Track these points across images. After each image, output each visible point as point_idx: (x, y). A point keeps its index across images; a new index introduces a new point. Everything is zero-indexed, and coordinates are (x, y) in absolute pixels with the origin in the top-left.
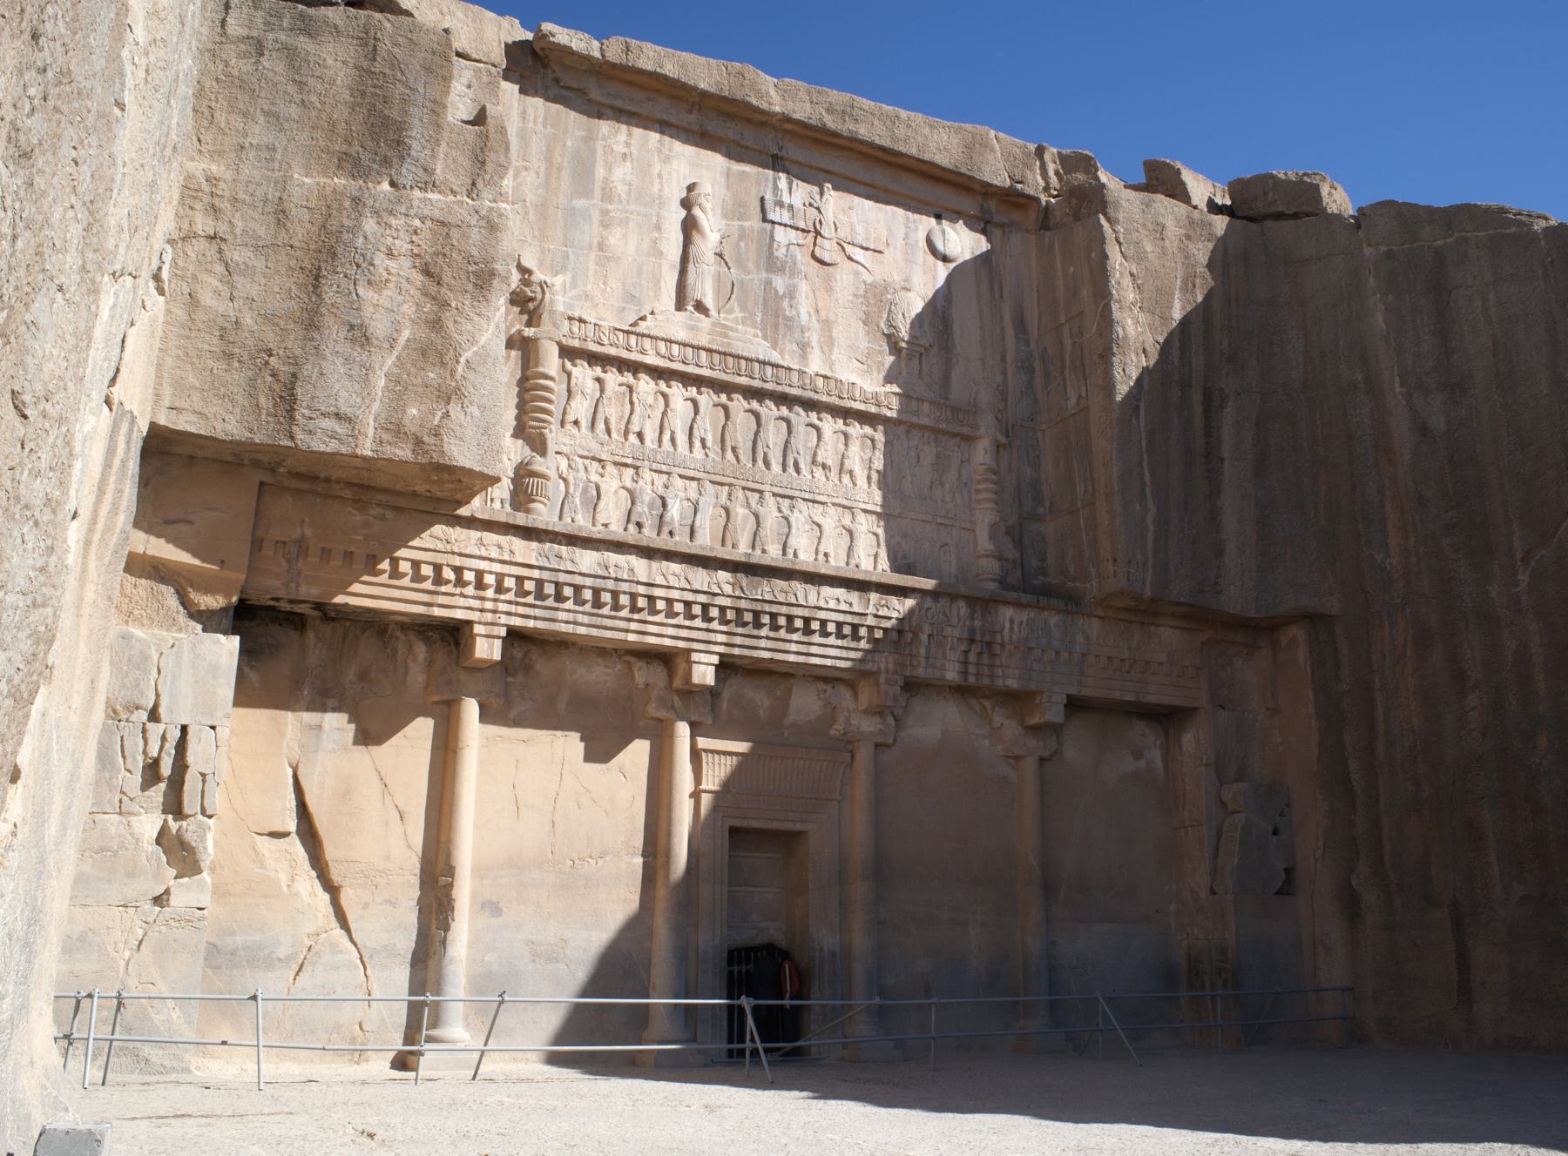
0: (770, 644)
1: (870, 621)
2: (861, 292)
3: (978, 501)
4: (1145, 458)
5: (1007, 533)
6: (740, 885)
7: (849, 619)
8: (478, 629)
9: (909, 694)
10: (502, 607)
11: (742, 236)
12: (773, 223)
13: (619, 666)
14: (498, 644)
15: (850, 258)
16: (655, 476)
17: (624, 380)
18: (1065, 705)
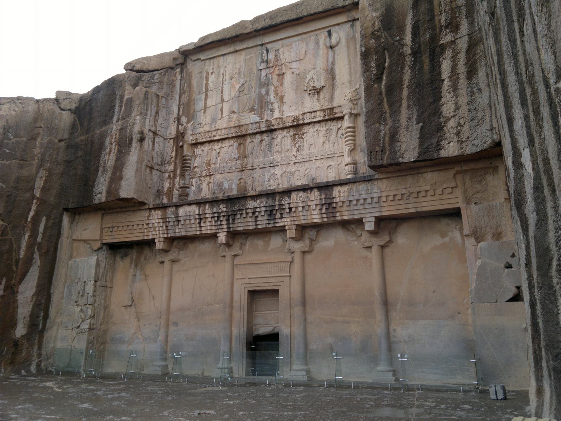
0: (242, 225)
1: (277, 207)
2: (295, 79)
3: (346, 142)
4: (385, 100)
5: (361, 151)
6: (266, 311)
7: (268, 209)
8: (156, 240)
9: (317, 230)
10: (161, 232)
11: (250, 81)
12: (261, 70)
13: (213, 241)
14: (161, 243)
15: (290, 68)
16: (220, 176)
17: (210, 147)
18: (375, 222)
